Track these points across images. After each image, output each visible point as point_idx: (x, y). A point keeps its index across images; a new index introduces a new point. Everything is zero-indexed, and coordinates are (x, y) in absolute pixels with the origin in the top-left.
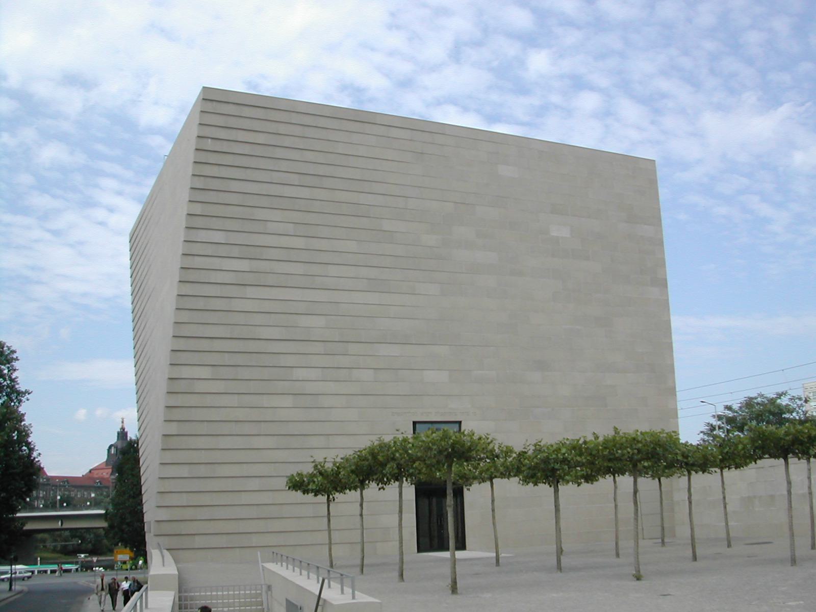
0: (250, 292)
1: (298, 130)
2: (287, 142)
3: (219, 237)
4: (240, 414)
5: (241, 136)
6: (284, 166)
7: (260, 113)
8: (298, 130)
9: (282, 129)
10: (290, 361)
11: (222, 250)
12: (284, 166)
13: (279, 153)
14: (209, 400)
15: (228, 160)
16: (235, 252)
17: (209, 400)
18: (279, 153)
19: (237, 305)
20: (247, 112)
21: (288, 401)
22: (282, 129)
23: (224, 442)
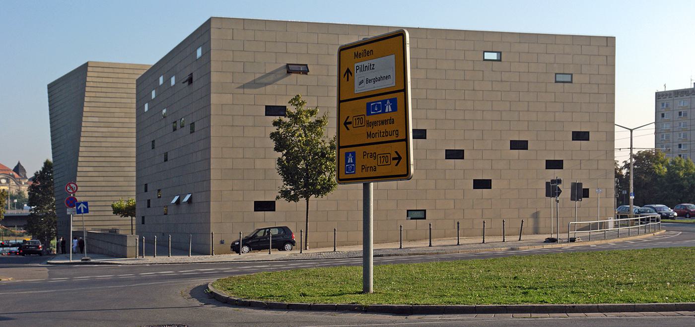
0: (109, 139)
1: (126, 76)
2: (121, 81)
3: (96, 119)
4: (104, 184)
5: (104, 80)
6: (121, 90)
7: (111, 70)
8: (126, 76)
9: (120, 76)
10: (123, 164)
11: (98, 125)
12: (121, 90)
13: (119, 86)
14: (92, 179)
15: (99, 90)
16: (102, 125)
17: (92, 179)
18: (119, 86)
19: (104, 144)
20: (106, 70)
21: (122, 179)
22: (120, 76)
23: (98, 194)
